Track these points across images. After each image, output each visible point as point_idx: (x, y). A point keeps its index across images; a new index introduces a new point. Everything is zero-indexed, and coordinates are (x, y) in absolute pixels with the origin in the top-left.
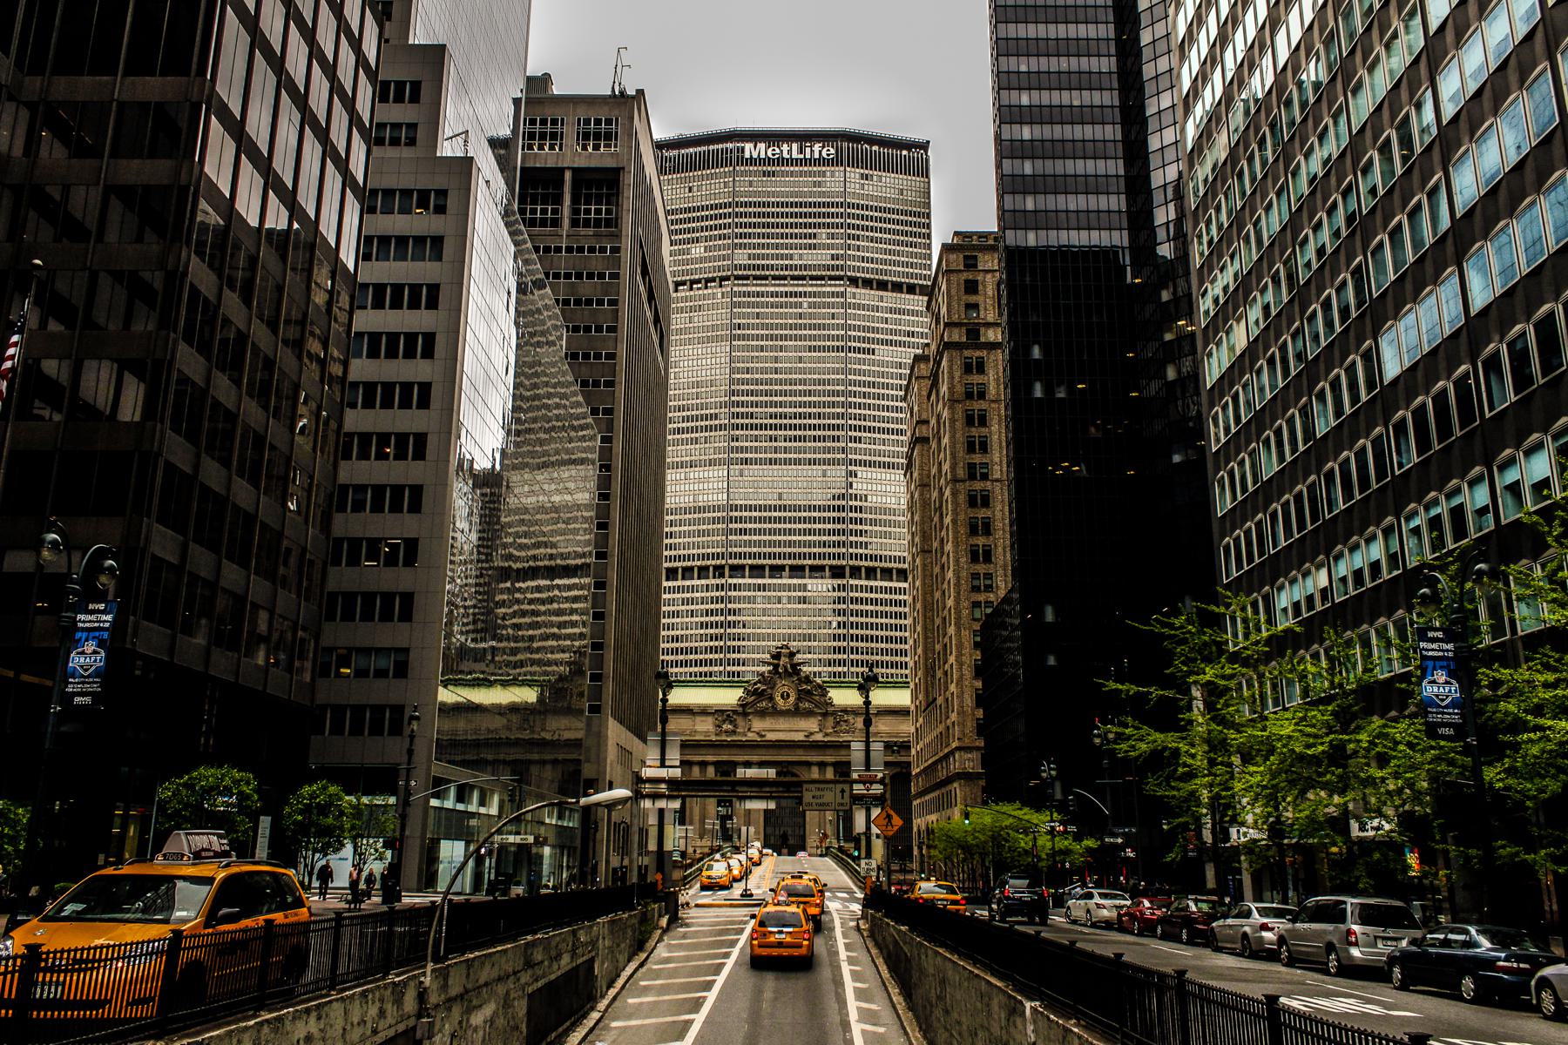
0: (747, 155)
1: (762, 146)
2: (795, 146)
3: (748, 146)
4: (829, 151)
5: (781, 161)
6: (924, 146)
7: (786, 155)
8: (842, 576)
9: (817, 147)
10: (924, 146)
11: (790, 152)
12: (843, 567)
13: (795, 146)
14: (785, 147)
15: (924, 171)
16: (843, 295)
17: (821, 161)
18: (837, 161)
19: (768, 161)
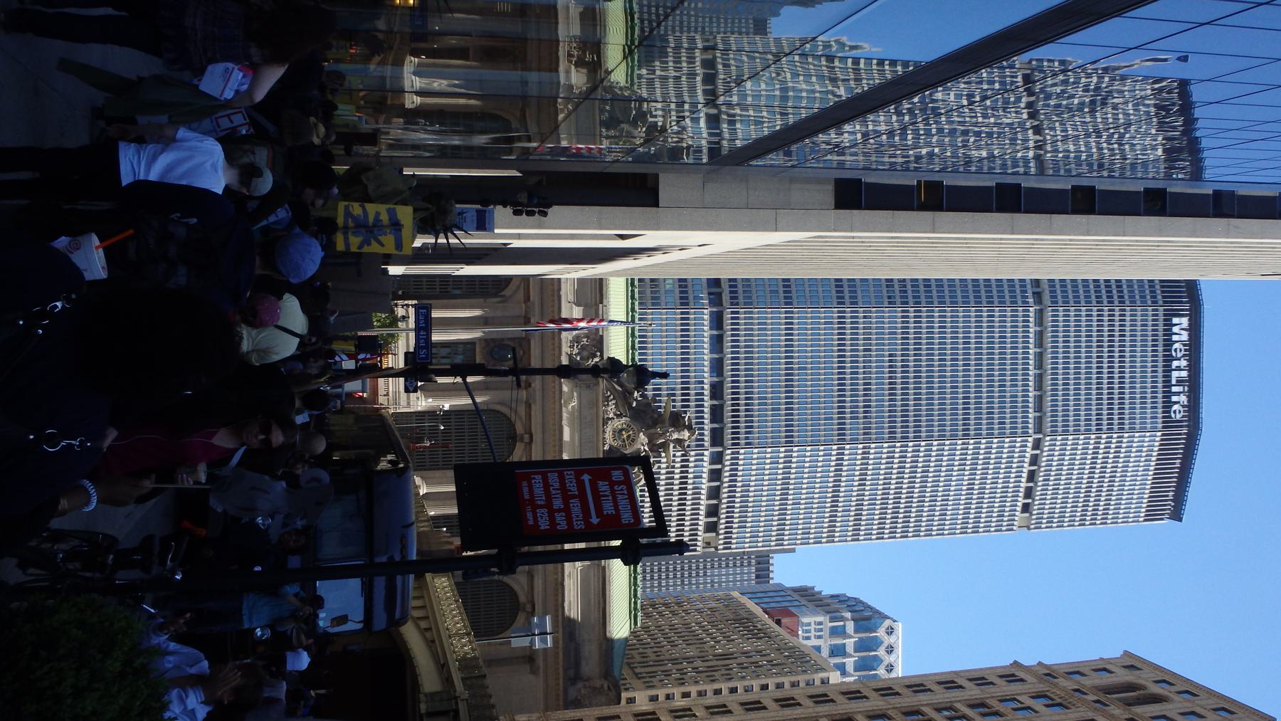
0: (1175, 320)
1: (1185, 336)
2: (1184, 374)
3: (1185, 321)
4: (1178, 412)
5: (1169, 359)
6: (1177, 515)
7: (1175, 364)
8: (713, 444)
9: (1183, 399)
10: (1177, 515)
11: (1178, 369)
12: (721, 444)
13: (1184, 374)
14: (1184, 363)
15: (1150, 516)
16: (1025, 434)
17: (1168, 405)
18: (1168, 423)
19: (1168, 344)
